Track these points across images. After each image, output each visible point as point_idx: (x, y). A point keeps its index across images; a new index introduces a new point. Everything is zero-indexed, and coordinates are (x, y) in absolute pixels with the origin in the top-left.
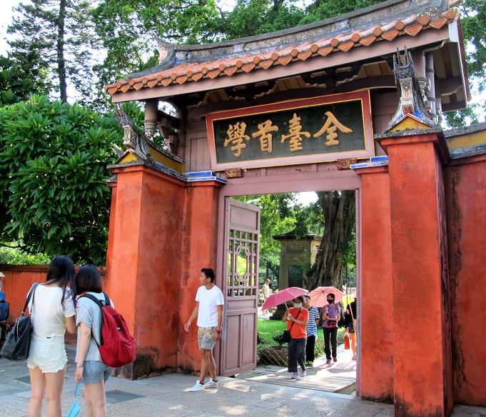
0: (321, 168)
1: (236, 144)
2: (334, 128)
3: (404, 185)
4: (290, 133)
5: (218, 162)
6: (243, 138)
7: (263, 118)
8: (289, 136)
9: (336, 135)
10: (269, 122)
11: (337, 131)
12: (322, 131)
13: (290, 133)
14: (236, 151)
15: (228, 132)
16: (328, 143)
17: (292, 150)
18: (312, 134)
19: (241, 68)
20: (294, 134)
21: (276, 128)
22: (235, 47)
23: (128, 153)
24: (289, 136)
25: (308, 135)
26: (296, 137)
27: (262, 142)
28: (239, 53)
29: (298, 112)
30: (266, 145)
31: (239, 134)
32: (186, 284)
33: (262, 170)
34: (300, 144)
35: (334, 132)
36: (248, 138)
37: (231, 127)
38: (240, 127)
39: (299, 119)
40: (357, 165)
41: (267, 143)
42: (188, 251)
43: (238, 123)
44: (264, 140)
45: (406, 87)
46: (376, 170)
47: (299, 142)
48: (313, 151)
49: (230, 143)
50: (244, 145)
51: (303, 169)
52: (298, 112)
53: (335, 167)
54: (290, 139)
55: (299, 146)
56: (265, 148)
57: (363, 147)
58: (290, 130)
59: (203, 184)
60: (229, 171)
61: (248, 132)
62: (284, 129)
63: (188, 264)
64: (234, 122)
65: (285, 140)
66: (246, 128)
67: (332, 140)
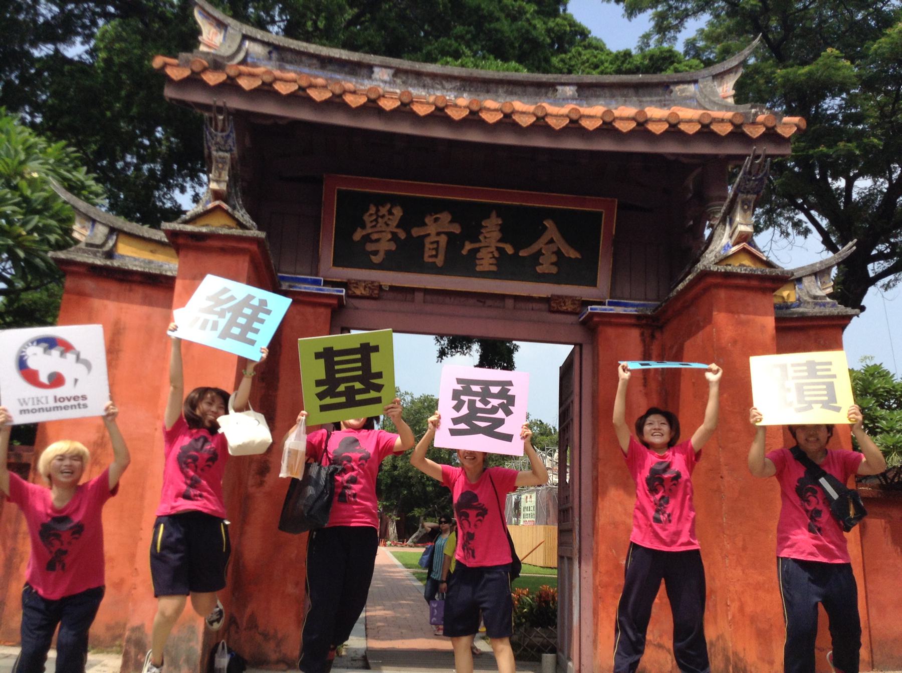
1: (378, 240)
2: (553, 247)
3: (735, 342)
4: (480, 241)
5: (336, 263)
6: (394, 234)
7: (437, 207)
8: (476, 245)
9: (554, 259)
10: (445, 217)
11: (558, 253)
12: (534, 248)
13: (480, 241)
14: (376, 253)
15: (366, 218)
16: (539, 269)
17: (478, 269)
18: (517, 248)
20: (486, 245)
21: (456, 229)
24: (476, 245)
25: (509, 250)
26: (490, 250)
27: (428, 246)
30: (434, 253)
31: (388, 225)
32: (261, 484)
33: (417, 294)
34: (493, 261)
35: (553, 253)
36: (402, 235)
37: (373, 210)
38: (390, 213)
39: (500, 222)
41: (437, 249)
43: (388, 206)
44: (432, 243)
45: (746, 207)
47: (494, 257)
49: (367, 239)
50: (393, 246)
51: (489, 302)
52: (501, 211)
53: (544, 306)
54: (477, 250)
55: (491, 264)
57: (593, 283)
58: (481, 238)
60: (357, 283)
62: (472, 232)
64: (380, 200)
65: (470, 251)
67: (546, 266)
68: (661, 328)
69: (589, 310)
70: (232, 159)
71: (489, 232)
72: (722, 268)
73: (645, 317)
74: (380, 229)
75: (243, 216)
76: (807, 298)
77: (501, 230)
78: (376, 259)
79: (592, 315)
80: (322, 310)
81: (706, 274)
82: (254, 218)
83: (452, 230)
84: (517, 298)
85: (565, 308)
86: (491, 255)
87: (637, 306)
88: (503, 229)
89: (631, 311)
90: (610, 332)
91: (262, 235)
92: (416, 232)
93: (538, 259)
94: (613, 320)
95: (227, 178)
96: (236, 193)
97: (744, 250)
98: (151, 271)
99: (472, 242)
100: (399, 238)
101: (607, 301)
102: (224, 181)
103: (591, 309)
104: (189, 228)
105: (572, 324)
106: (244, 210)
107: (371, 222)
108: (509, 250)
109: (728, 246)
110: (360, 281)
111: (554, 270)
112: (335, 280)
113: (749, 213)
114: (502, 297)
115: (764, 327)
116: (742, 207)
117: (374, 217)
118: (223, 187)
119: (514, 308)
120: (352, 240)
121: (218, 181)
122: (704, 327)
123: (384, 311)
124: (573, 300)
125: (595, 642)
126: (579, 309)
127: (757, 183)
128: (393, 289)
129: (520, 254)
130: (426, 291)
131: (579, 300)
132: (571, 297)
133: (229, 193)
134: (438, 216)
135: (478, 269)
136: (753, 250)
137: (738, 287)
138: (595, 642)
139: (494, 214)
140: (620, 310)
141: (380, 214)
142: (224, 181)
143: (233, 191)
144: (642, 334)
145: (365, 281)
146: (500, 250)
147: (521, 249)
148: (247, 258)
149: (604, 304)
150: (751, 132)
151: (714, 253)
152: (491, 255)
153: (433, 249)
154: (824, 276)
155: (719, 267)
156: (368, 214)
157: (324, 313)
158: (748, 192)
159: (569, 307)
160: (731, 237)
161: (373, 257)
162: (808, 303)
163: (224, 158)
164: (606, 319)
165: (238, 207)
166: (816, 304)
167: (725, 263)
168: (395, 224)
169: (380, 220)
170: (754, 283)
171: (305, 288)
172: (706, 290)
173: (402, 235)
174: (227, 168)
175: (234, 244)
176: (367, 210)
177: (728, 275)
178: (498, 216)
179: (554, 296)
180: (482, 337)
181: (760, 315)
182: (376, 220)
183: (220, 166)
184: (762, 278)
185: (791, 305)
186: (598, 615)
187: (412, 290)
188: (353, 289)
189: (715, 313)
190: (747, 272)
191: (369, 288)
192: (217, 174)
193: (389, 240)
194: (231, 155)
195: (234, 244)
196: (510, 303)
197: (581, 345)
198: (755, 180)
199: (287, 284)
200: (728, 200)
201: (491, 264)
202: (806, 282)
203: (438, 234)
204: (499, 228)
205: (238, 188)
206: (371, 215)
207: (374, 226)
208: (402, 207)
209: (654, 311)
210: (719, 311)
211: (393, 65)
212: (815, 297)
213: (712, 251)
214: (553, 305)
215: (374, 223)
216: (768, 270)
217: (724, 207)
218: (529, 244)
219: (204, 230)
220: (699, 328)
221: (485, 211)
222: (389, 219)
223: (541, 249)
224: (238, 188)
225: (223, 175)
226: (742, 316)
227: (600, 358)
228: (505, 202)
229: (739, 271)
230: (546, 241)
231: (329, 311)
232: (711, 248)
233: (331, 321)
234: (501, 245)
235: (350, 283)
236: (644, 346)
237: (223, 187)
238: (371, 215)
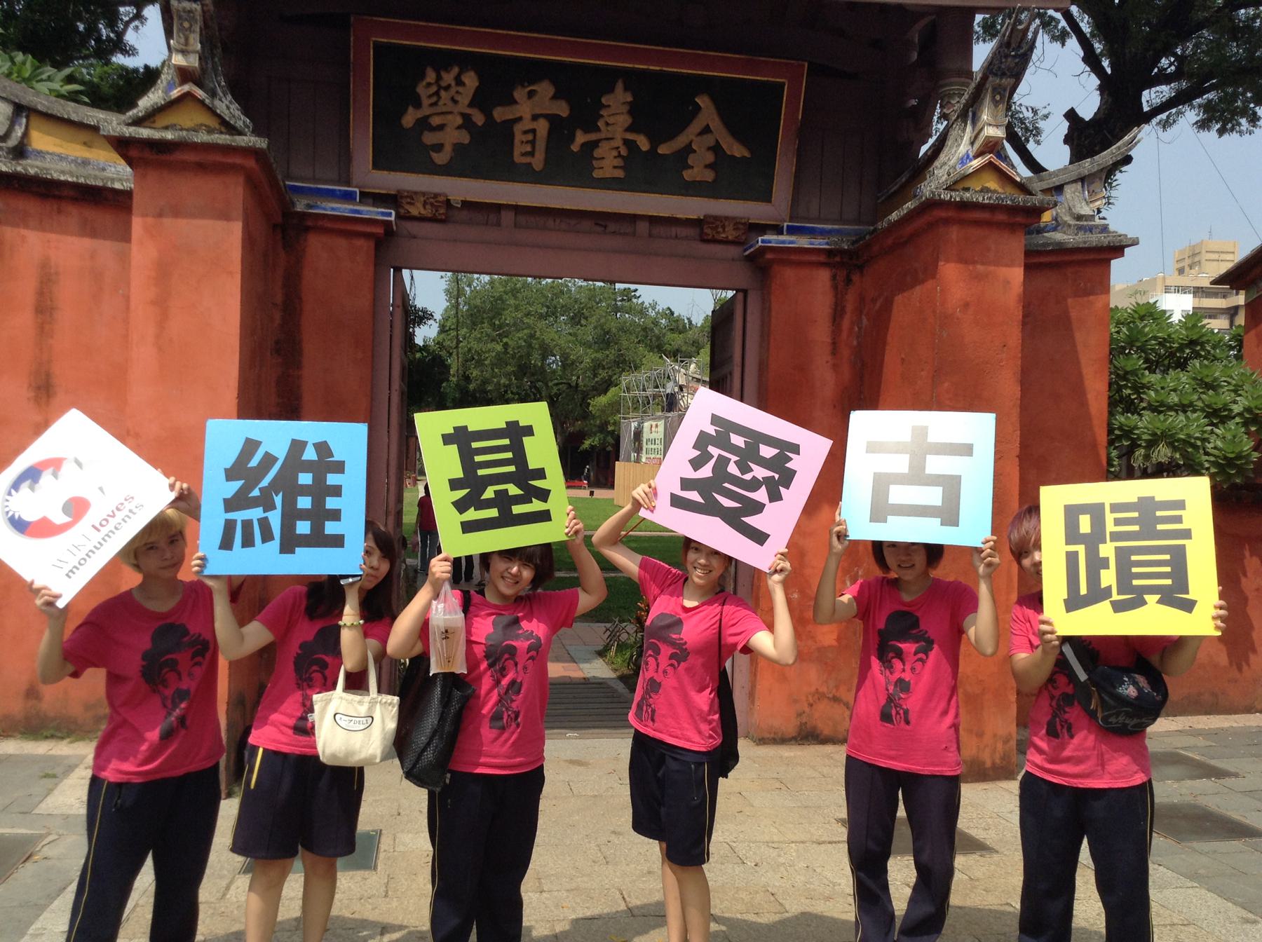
1: (441, 127)
2: (709, 140)
4: (598, 130)
5: (376, 166)
7: (532, 72)
8: (593, 137)
9: (710, 158)
10: (545, 89)
11: (716, 149)
12: (680, 142)
14: (439, 148)
15: (421, 89)
16: (688, 175)
17: (597, 174)
18: (655, 141)
20: (610, 136)
21: (562, 109)
24: (593, 137)
25: (643, 143)
27: (519, 137)
30: (529, 148)
31: (455, 101)
34: (619, 162)
35: (709, 149)
36: (479, 119)
37: (431, 76)
38: (459, 82)
39: (629, 98)
41: (533, 143)
43: (456, 70)
44: (526, 132)
45: (998, 97)
47: (620, 156)
49: (423, 124)
50: (465, 138)
51: (612, 227)
52: (634, 80)
53: (691, 232)
54: (595, 144)
55: (615, 167)
56: (525, 154)
58: (601, 124)
59: (344, 228)
60: (412, 196)
61: (482, 100)
62: (587, 116)
64: (442, 61)
65: (583, 145)
66: (478, 89)
67: (697, 171)
68: (861, 268)
69: (760, 244)
70: (203, 11)
71: (613, 115)
72: (956, 196)
73: (841, 252)
74: (444, 109)
75: (228, 108)
76: (1067, 218)
77: (630, 112)
78: (440, 158)
79: (763, 250)
80: (360, 243)
81: (933, 204)
82: (246, 112)
83: (558, 113)
84: (653, 220)
85: (724, 235)
87: (830, 232)
88: (633, 110)
89: (820, 243)
90: (789, 274)
91: (261, 143)
92: (500, 114)
94: (793, 257)
95: (199, 46)
96: (215, 70)
97: (990, 166)
98: (89, 182)
99: (586, 131)
100: (474, 124)
101: (785, 224)
102: (195, 52)
103: (763, 241)
104: (144, 133)
105: (733, 260)
106: (229, 97)
107: (430, 96)
108: (643, 143)
109: (968, 156)
110: (416, 193)
111: (709, 176)
112: (377, 191)
113: (1002, 107)
114: (634, 218)
115: (1008, 282)
116: (993, 98)
117: (434, 89)
118: (193, 62)
119: (650, 236)
120: (401, 126)
121: (184, 52)
122: (923, 282)
123: (455, 241)
124: (736, 224)
125: (751, 695)
126: (744, 238)
127: (1017, 60)
128: (467, 205)
129: (660, 151)
130: (518, 209)
131: (744, 224)
132: (734, 218)
133: (203, 70)
135: (597, 174)
136: (1003, 165)
137: (977, 223)
138: (751, 695)
139: (620, 86)
140: (803, 242)
141: (443, 84)
142: (195, 52)
143: (210, 66)
144: (834, 277)
145: (424, 194)
147: (661, 143)
148: (241, 180)
149: (781, 233)
151: (947, 168)
152: (615, 153)
153: (527, 142)
154: (1093, 183)
155: (953, 194)
156: (424, 83)
157: (365, 246)
158: (1004, 74)
159: (731, 234)
160: (972, 143)
161: (434, 155)
162: (1070, 226)
163: (191, 11)
164: (785, 257)
165: (219, 91)
166: (1080, 228)
167: (961, 186)
168: (467, 101)
169: (443, 93)
170: (1001, 217)
171: (333, 209)
172: (932, 225)
173: (479, 119)
174: (198, 30)
175: (219, 158)
176: (423, 76)
177: (964, 206)
178: (626, 89)
181: (1007, 266)
182: (437, 93)
183: (186, 25)
184: (1014, 210)
185: (1046, 226)
186: (757, 664)
187: (498, 208)
188: (407, 207)
189: (941, 263)
190: (992, 202)
191: (432, 204)
192: (182, 40)
193: (459, 128)
194: (203, 5)
195: (219, 158)
196: (643, 227)
197: (745, 292)
198: (1014, 57)
199: (305, 202)
200: (973, 85)
201: (615, 167)
202: (1069, 191)
203: (535, 118)
204: (625, 109)
205: (216, 59)
206: (429, 85)
207: (435, 104)
208: (476, 72)
209: (854, 243)
210: (947, 261)
212: (1079, 217)
213: (945, 164)
214: (708, 231)
215: (434, 99)
216: (1021, 198)
217: (966, 96)
218: (671, 136)
219: (169, 136)
220: (917, 281)
221: (606, 79)
222: (457, 92)
224: (216, 59)
225: (191, 41)
226: (980, 268)
227: (773, 314)
228: (637, 66)
229: (980, 199)
230: (699, 131)
231: (372, 244)
232: (942, 157)
233: (376, 256)
234: (630, 136)
235: (402, 197)
236: (836, 296)
237: (193, 62)
238: (429, 85)
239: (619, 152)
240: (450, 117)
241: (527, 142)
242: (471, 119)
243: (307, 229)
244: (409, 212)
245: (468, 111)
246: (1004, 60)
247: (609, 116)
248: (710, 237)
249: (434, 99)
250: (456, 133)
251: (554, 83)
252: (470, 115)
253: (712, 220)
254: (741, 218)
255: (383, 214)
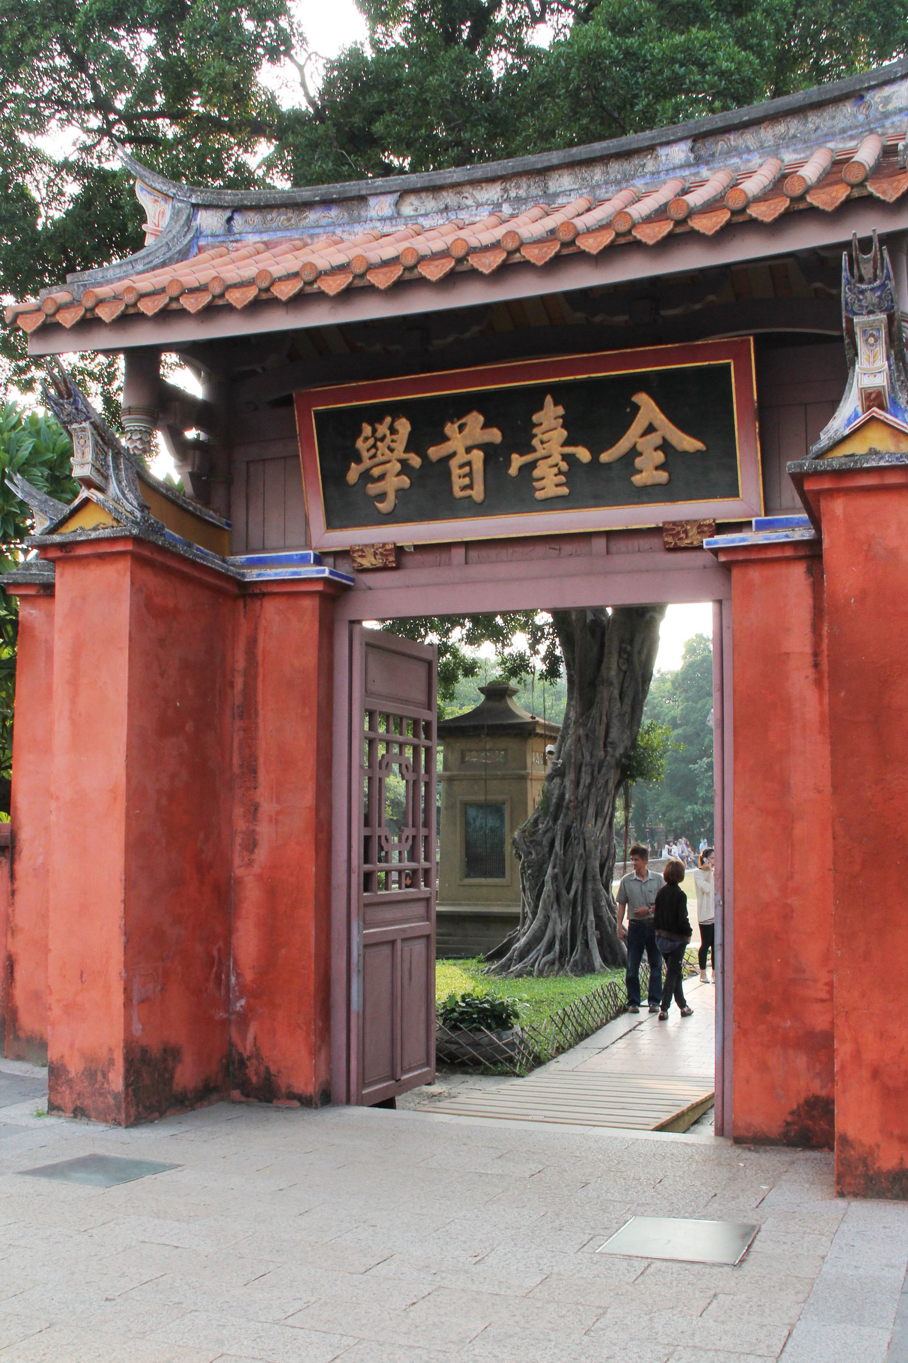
0: (620, 545)
1: (382, 477)
2: (655, 439)
3: (863, 596)
4: (533, 450)
5: (331, 525)
8: (529, 458)
9: (660, 457)
10: (475, 420)
11: (665, 446)
13: (533, 450)
14: (382, 497)
15: (360, 444)
16: (637, 479)
17: (539, 495)
18: (595, 454)
19: (415, 266)
21: (495, 435)
22: (372, 201)
23: (87, 501)
24: (529, 458)
25: (583, 454)
26: (550, 461)
27: (456, 472)
28: (383, 219)
29: (560, 393)
30: (467, 481)
31: (392, 450)
34: (562, 479)
36: (415, 461)
37: (367, 430)
38: (393, 430)
39: (560, 410)
40: (723, 540)
41: (470, 475)
42: (251, 769)
43: (388, 420)
44: (461, 466)
45: (871, 340)
46: (770, 554)
47: (560, 473)
48: (598, 500)
49: (366, 477)
50: (405, 482)
51: (568, 548)
53: (655, 542)
54: (533, 465)
55: (557, 485)
56: (463, 488)
57: (732, 491)
58: (535, 442)
60: (362, 550)
61: (415, 444)
63: (253, 811)
64: (375, 415)
65: (521, 469)
66: (411, 434)
78: (384, 507)
84: (610, 535)
85: (689, 541)
86: (555, 470)
93: (633, 464)
99: (521, 455)
100: (413, 468)
105: (705, 567)
107: (368, 450)
110: (366, 546)
111: (662, 477)
117: (371, 441)
119: (608, 552)
120: (346, 484)
124: (700, 526)
127: (878, 294)
128: (417, 548)
131: (710, 525)
132: (695, 521)
134: (460, 422)
139: (549, 399)
141: (379, 434)
145: (373, 545)
146: (568, 458)
150: (884, 193)
152: (555, 470)
156: (361, 439)
158: (871, 312)
161: (380, 506)
164: (740, 557)
169: (379, 444)
171: (276, 575)
176: (359, 432)
178: (556, 404)
179: (669, 523)
180: (556, 608)
182: (374, 446)
187: (448, 546)
188: (359, 560)
193: (398, 475)
207: (374, 456)
208: (408, 419)
211: (394, 188)
218: (612, 442)
223: (635, 445)
235: (354, 552)
238: (366, 439)
239: (559, 469)
240: (388, 465)
241: (464, 476)
242: (408, 465)
243: (264, 595)
244: (362, 565)
245: (406, 456)
246: (861, 297)
247: (543, 433)
248: (672, 546)
249: (373, 451)
250: (396, 479)
251: (481, 412)
252: (407, 460)
253: (671, 526)
254: (704, 520)
255: (319, 572)
